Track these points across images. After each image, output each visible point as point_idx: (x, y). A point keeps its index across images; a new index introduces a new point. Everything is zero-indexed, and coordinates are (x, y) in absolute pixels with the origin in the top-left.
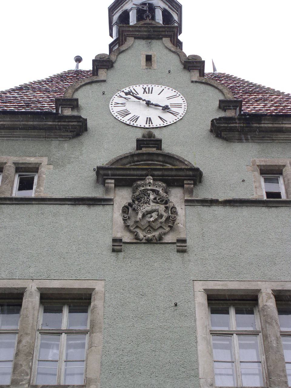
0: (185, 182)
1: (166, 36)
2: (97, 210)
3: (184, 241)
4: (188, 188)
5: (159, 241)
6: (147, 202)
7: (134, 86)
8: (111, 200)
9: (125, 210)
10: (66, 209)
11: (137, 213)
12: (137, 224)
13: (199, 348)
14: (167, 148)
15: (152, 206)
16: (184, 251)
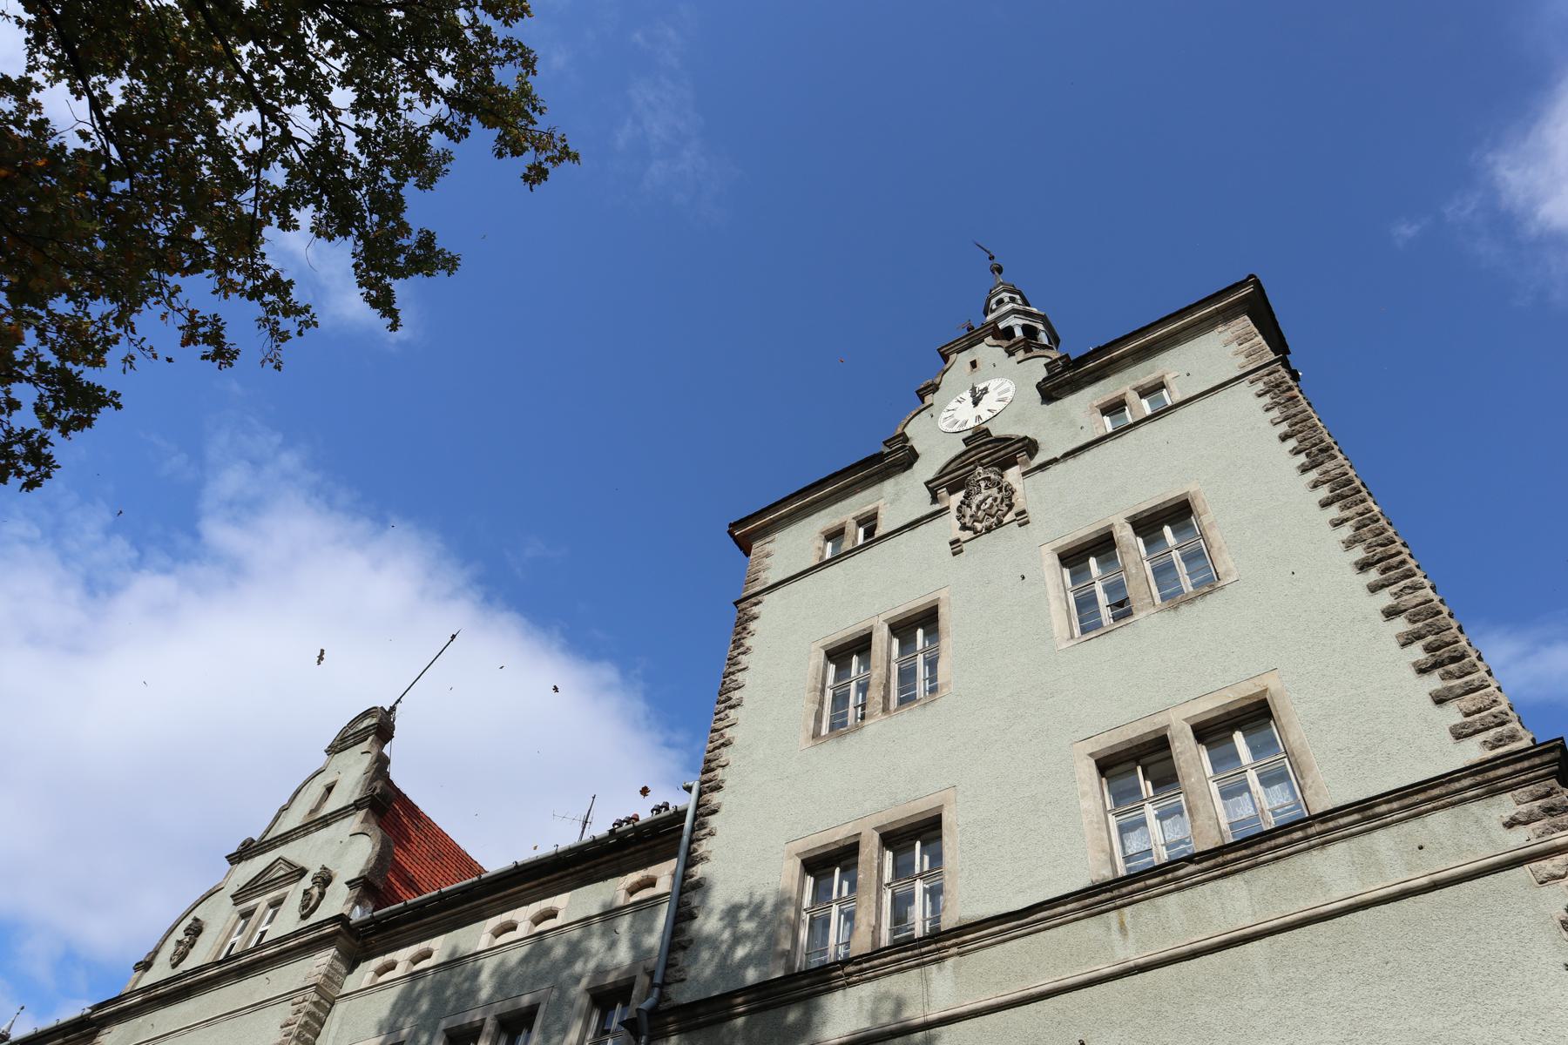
0: (1018, 456)
1: (987, 336)
2: (938, 522)
3: (1024, 512)
4: (1021, 462)
5: (1000, 524)
6: (979, 492)
7: (961, 396)
8: (948, 508)
9: (959, 509)
10: (907, 535)
11: (971, 508)
12: (974, 518)
13: (1052, 608)
14: (996, 432)
15: (985, 493)
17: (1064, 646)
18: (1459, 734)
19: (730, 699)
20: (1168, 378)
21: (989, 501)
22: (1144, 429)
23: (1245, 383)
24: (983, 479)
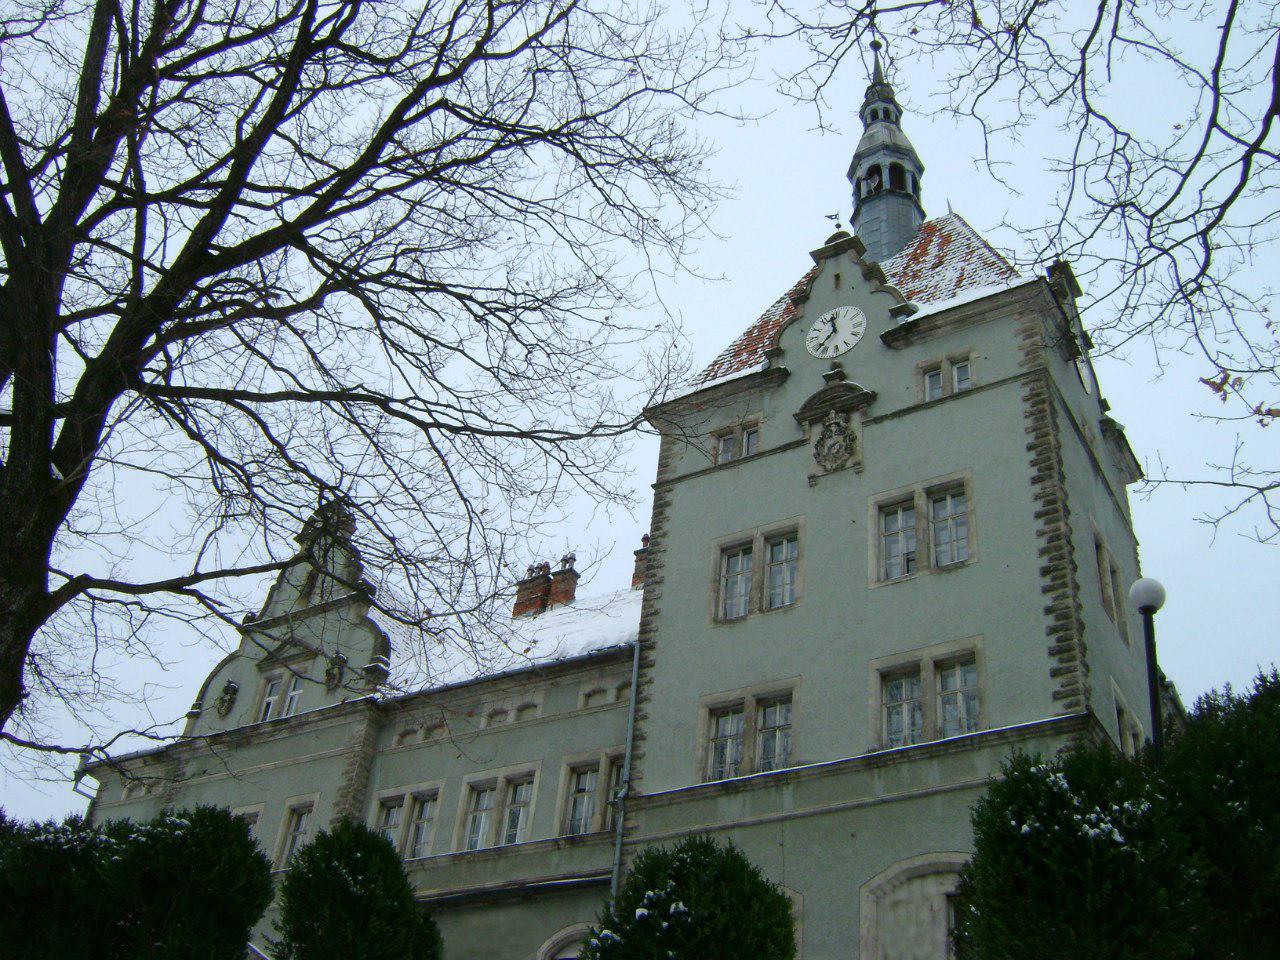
5: (841, 468)
10: (777, 457)
15: (836, 438)
16: (861, 471)
17: (872, 586)
18: (1056, 696)
19: (654, 575)
20: (973, 356)
21: (837, 446)
22: (950, 405)
23: (1017, 385)
24: (835, 423)
